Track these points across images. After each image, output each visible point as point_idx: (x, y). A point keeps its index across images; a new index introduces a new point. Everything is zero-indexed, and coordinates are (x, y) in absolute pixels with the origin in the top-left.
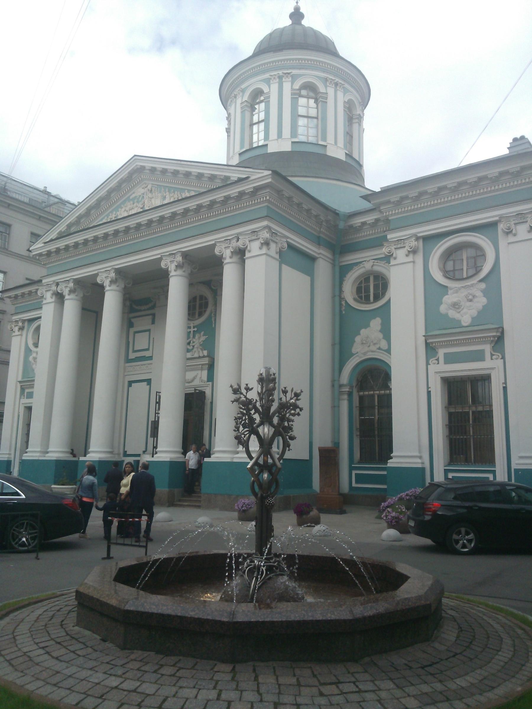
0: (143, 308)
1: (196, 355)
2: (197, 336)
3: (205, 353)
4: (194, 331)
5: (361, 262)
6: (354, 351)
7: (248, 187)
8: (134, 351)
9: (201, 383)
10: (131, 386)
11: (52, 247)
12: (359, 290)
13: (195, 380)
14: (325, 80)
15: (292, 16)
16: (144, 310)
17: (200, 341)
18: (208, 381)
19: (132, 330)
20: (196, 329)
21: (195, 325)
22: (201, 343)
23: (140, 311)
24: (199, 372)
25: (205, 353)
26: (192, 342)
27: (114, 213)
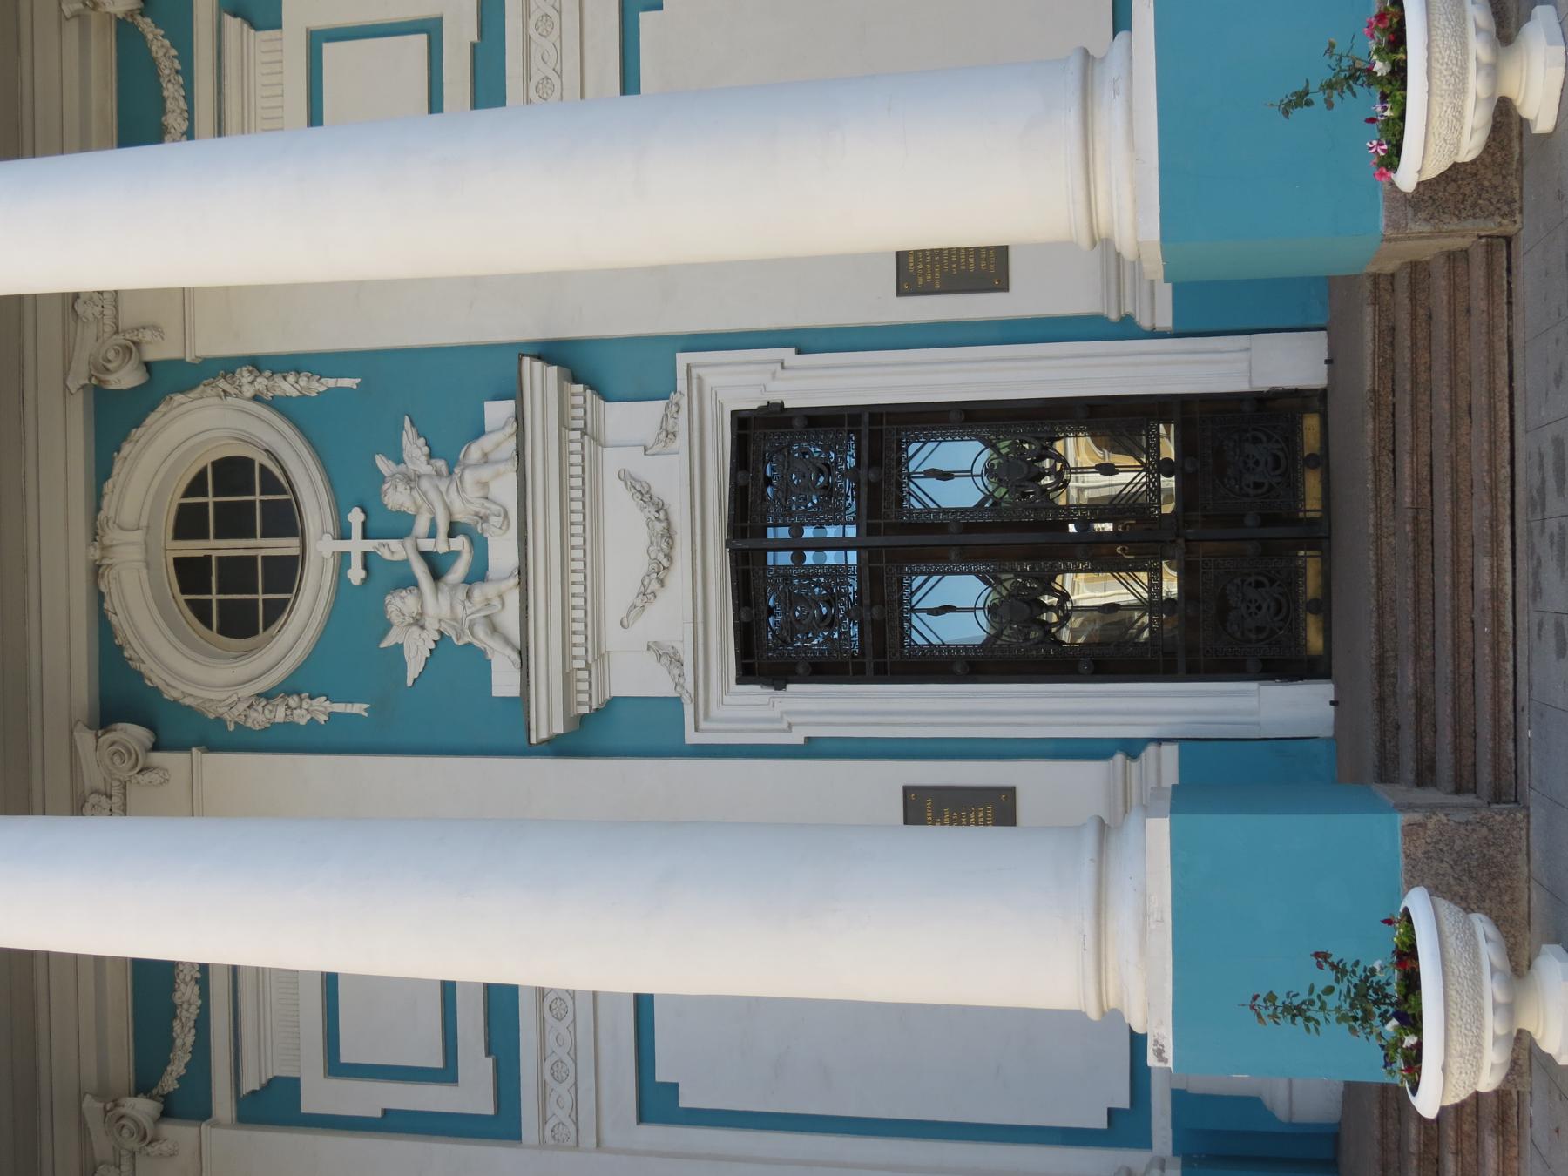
1: (505, 490)
2: (397, 497)
3: (498, 412)
4: (365, 536)
8: (447, 1073)
9: (682, 442)
13: (655, 491)
17: (423, 467)
18: (661, 389)
19: (319, 1095)
20: (356, 517)
21: (330, 527)
22: (441, 464)
23: (202, 1024)
24: (612, 461)
25: (498, 412)
26: (427, 545)
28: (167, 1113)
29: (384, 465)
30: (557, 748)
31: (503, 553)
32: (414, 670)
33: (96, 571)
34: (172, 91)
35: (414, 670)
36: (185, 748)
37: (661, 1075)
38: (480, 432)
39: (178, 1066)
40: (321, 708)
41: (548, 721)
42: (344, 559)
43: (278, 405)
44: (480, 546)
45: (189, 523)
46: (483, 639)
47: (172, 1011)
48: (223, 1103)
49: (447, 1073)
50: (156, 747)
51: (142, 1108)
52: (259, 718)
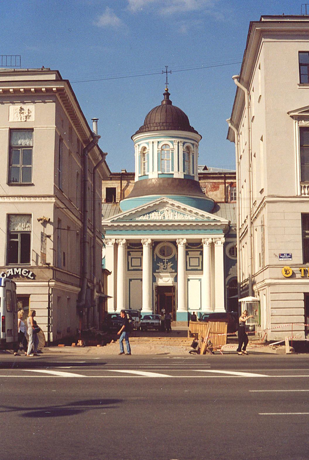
0: (136, 248)
2: (169, 264)
3: (174, 271)
5: (232, 242)
6: (229, 273)
7: (219, 224)
10: (131, 281)
11: (116, 224)
12: (230, 251)
14: (193, 144)
15: (164, 94)
16: (137, 249)
20: (167, 261)
23: (134, 249)
25: (174, 271)
27: (147, 215)
28: (128, 247)
29: (171, 262)
30: (153, 275)
31: (165, 271)
32: (158, 264)
33: (164, 242)
34: (196, 247)
35: (158, 264)
36: (153, 248)
37: (132, 281)
38: (173, 269)
39: (131, 246)
40: (155, 258)
41: (155, 274)
42: (165, 260)
43: (175, 255)
44: (166, 269)
45: (167, 247)
46: (160, 270)
47: (135, 246)
48: (129, 250)
49: (132, 266)
50: (153, 247)
51: (129, 245)
52: (155, 254)
